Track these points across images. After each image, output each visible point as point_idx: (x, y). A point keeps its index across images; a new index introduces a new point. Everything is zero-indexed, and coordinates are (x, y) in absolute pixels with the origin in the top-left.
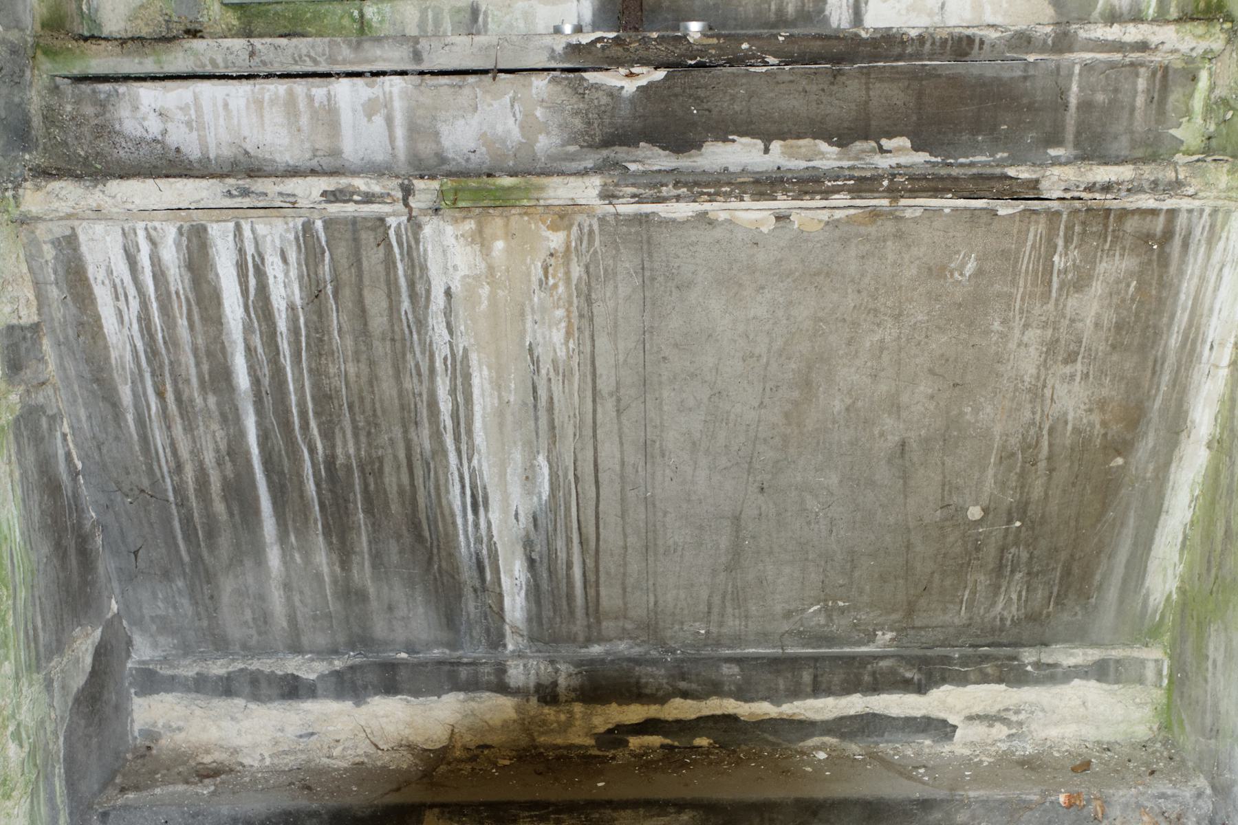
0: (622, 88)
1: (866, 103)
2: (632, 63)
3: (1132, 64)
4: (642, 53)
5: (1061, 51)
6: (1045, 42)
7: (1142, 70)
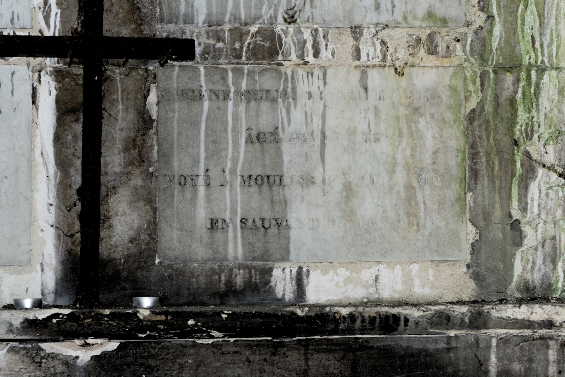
0: (77, 357)
1: (306, 371)
2: (86, 336)
3: (542, 338)
4: (95, 327)
5: (478, 328)
6: (462, 320)
7: (552, 343)
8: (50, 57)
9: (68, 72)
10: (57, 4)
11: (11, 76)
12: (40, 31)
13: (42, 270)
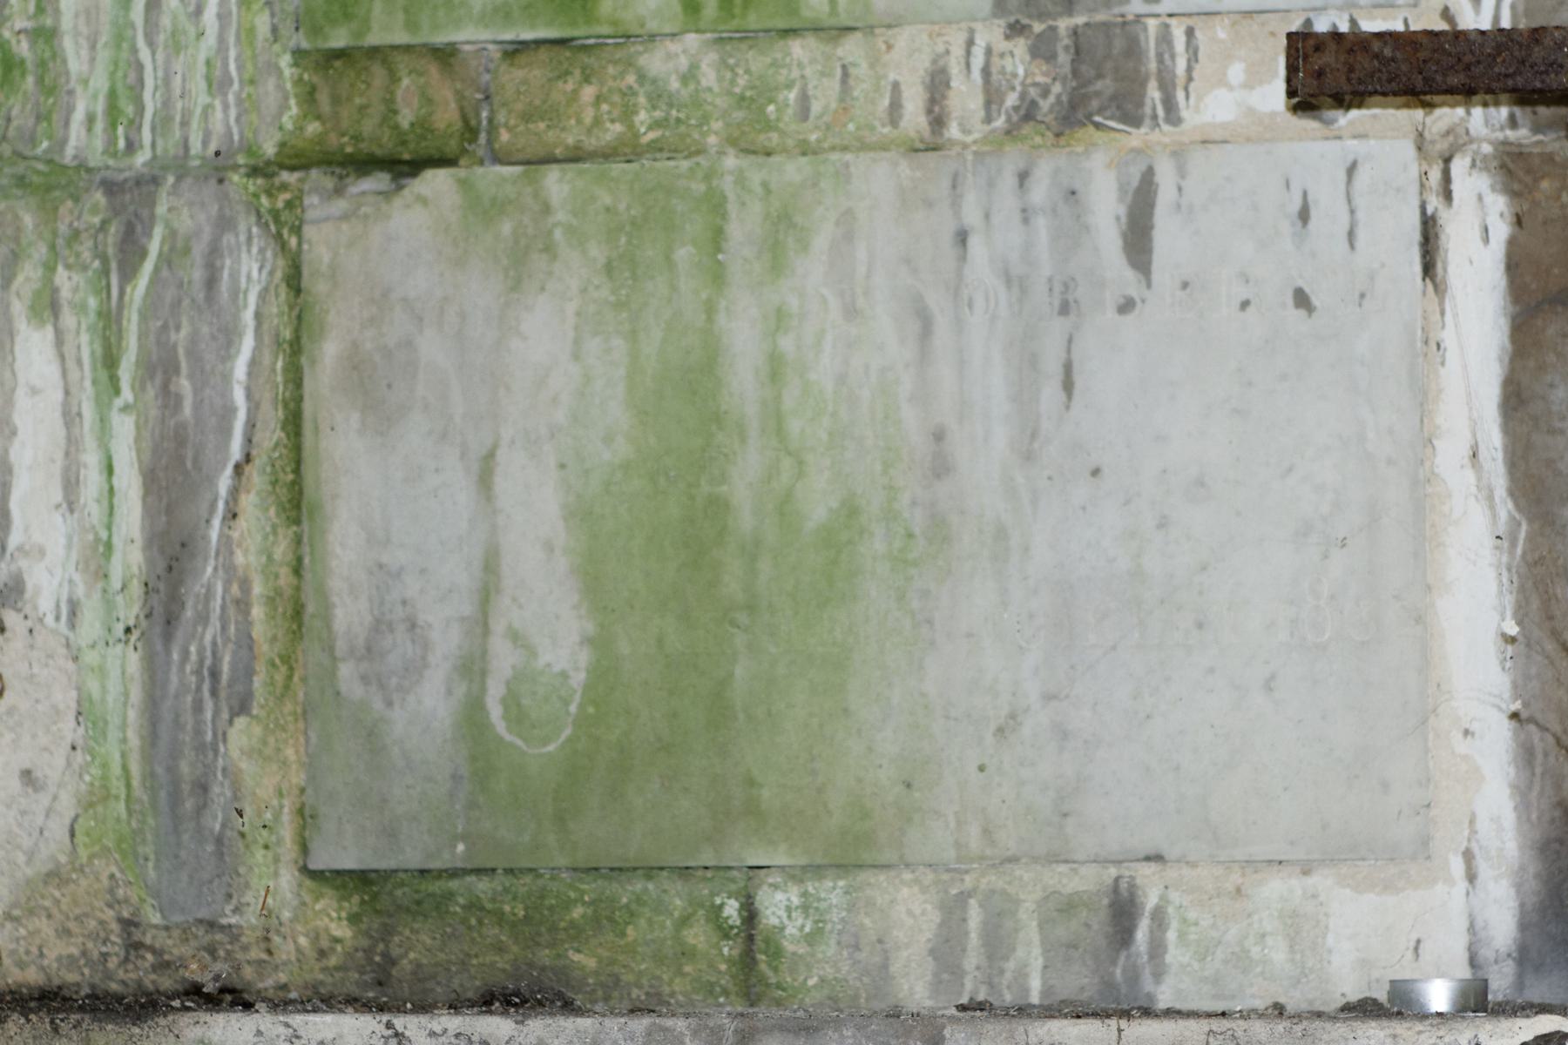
8: (1485, 105)
9: (1549, 158)
11: (1342, 176)
12: (1446, 14)
13: (1471, 877)
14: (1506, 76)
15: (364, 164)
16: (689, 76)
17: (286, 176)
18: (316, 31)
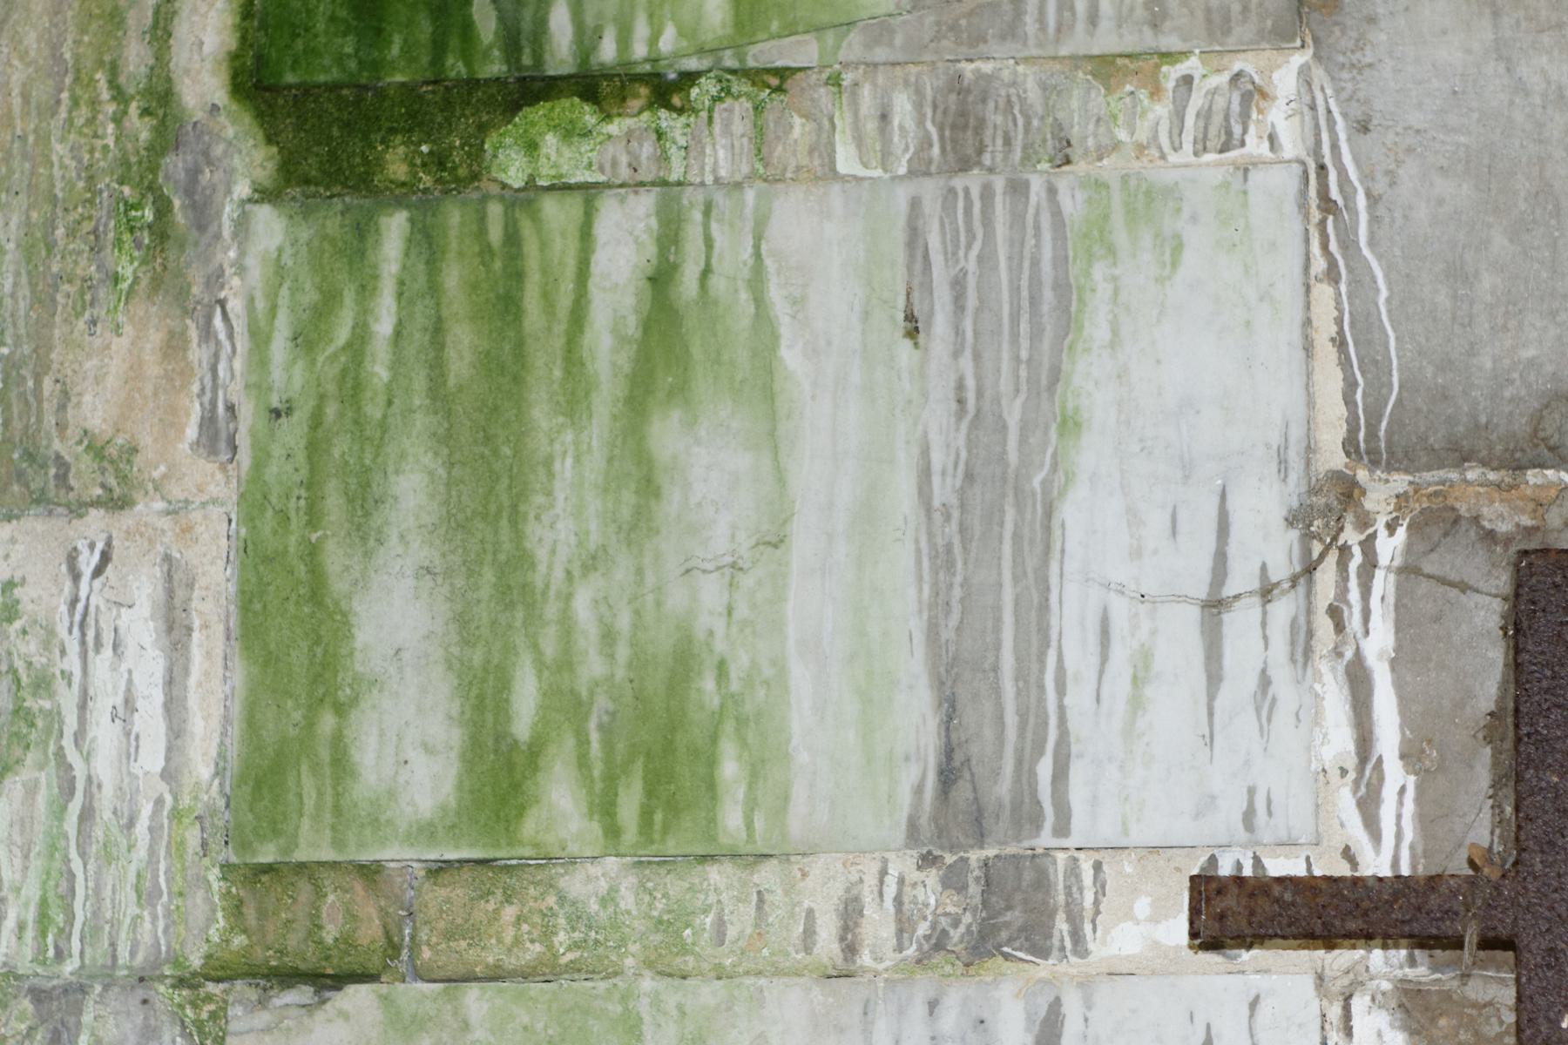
8: (1385, 947)
9: (1447, 996)
10: (1402, 757)
11: (1245, 1011)
12: (1348, 854)
14: (1403, 922)
15: (288, 977)
16: (608, 900)
17: (211, 987)
18: (244, 846)
